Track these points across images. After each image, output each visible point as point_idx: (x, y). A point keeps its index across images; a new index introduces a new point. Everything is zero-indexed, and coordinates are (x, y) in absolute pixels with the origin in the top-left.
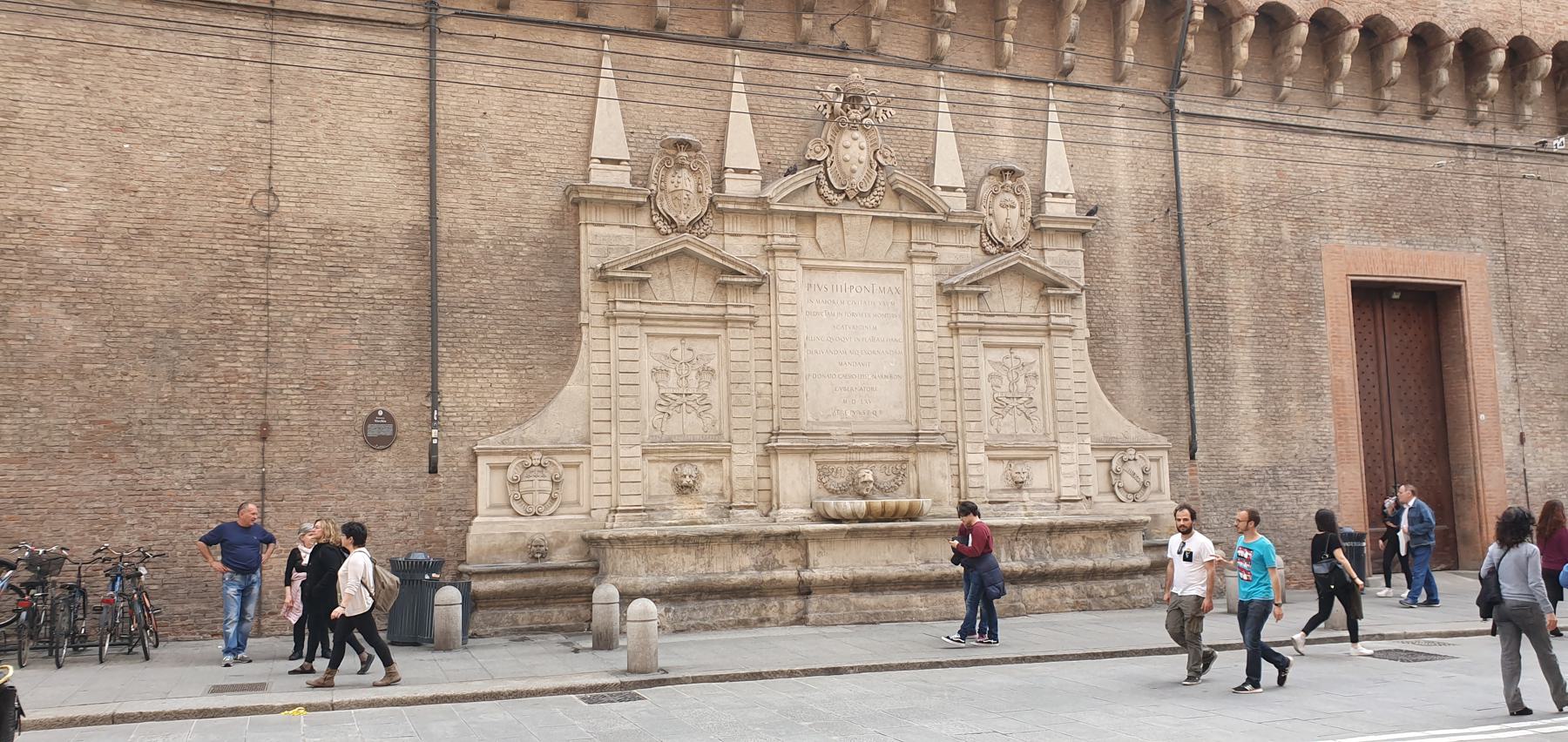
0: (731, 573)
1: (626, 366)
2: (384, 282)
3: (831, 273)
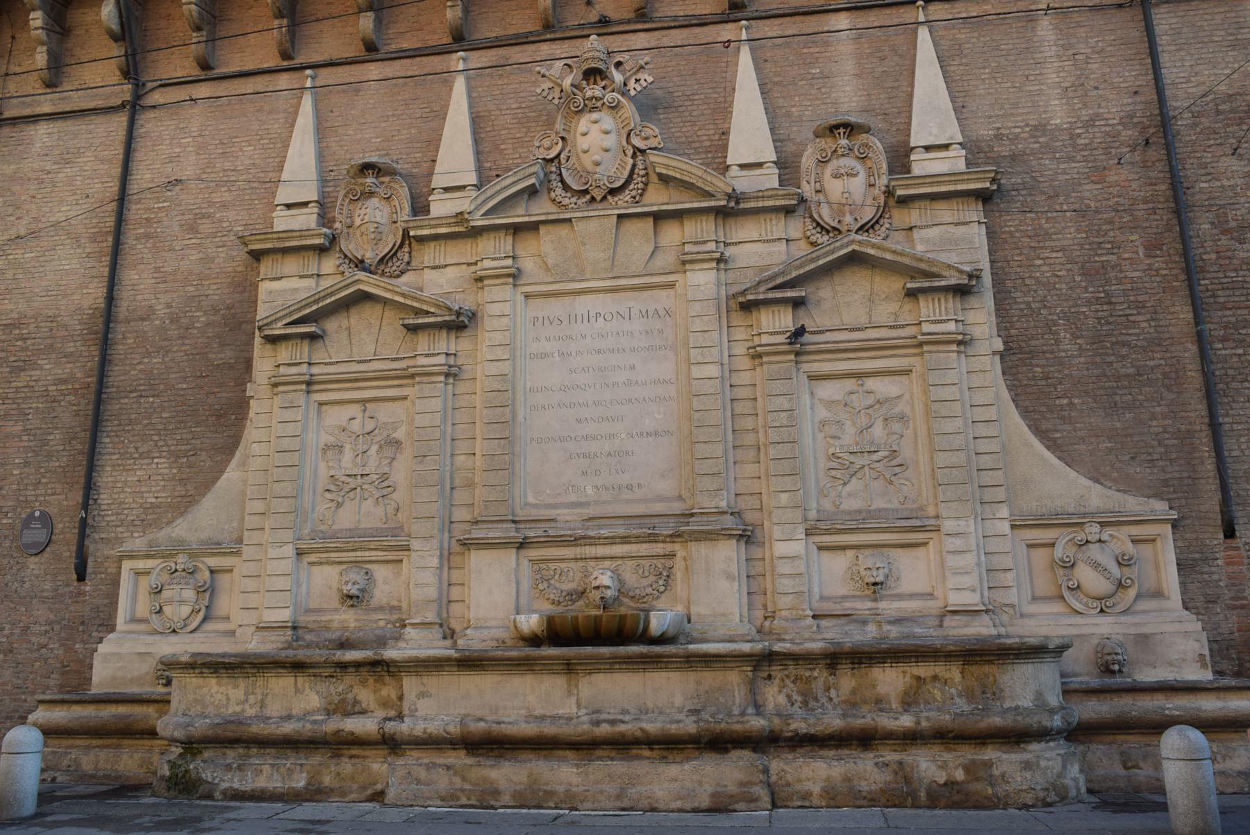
0: (289, 717)
1: (286, 444)
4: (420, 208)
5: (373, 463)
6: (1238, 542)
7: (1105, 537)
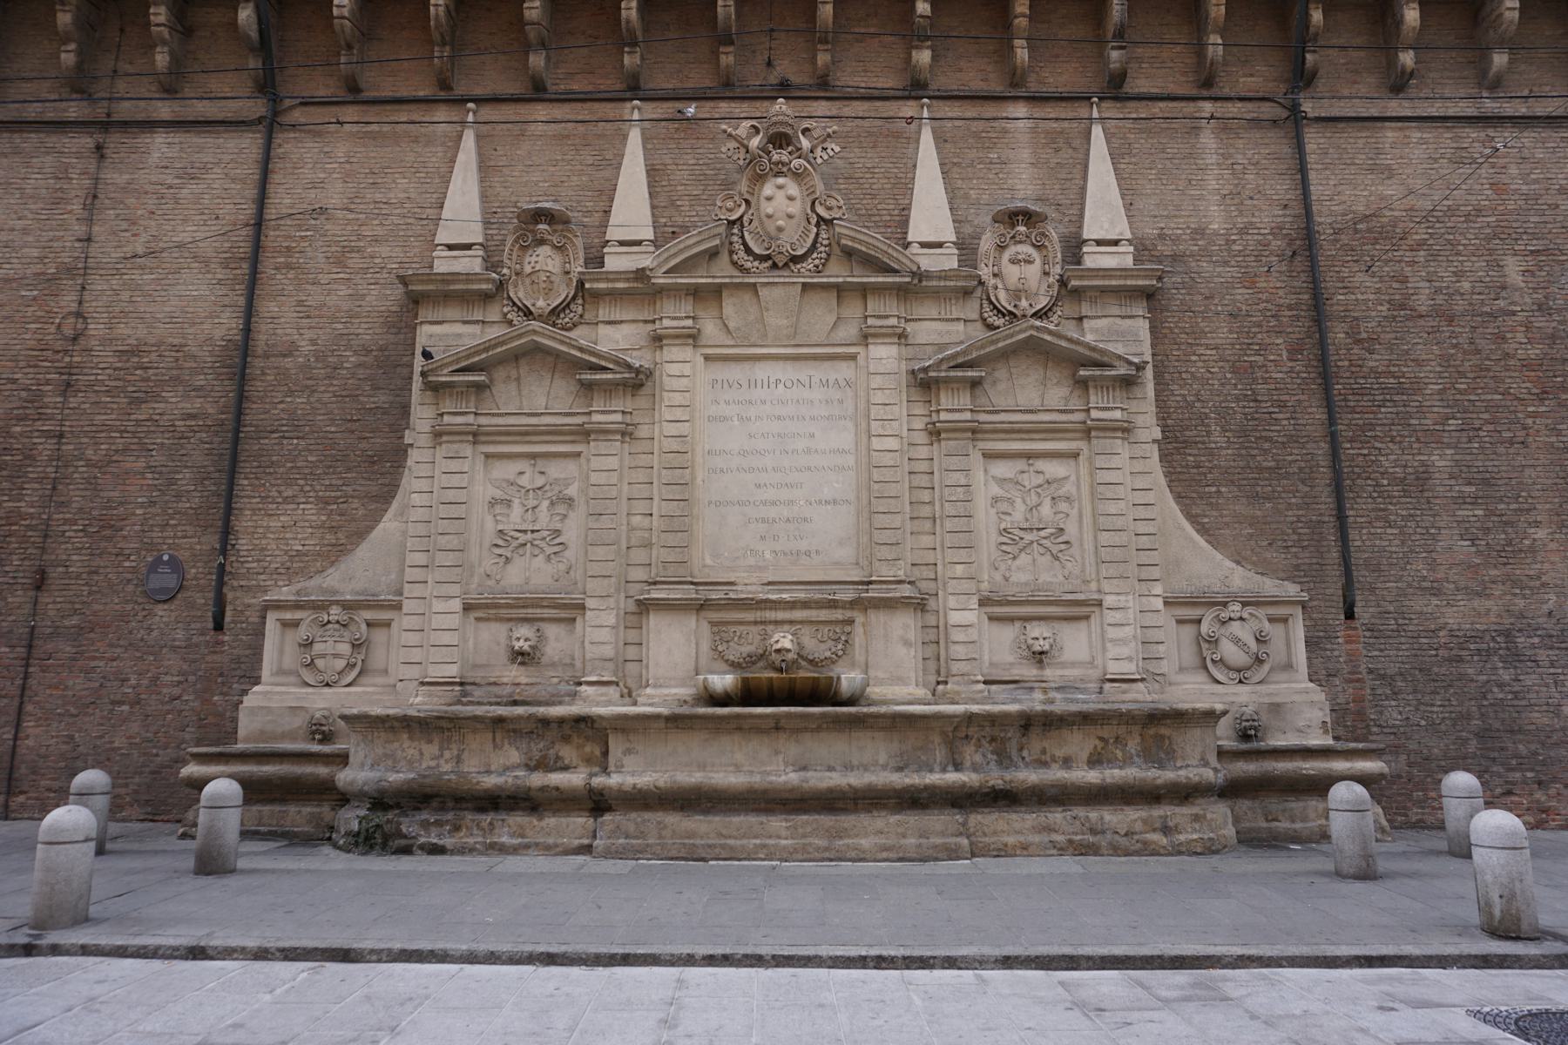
1: (451, 495)
2: (187, 406)
3: (747, 365)
4: (595, 260)
5: (544, 519)
6: (1357, 624)
7: (1245, 615)
